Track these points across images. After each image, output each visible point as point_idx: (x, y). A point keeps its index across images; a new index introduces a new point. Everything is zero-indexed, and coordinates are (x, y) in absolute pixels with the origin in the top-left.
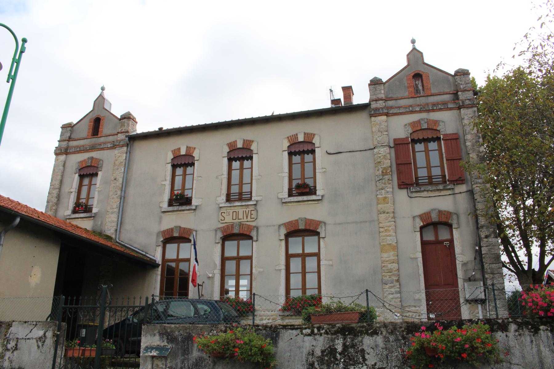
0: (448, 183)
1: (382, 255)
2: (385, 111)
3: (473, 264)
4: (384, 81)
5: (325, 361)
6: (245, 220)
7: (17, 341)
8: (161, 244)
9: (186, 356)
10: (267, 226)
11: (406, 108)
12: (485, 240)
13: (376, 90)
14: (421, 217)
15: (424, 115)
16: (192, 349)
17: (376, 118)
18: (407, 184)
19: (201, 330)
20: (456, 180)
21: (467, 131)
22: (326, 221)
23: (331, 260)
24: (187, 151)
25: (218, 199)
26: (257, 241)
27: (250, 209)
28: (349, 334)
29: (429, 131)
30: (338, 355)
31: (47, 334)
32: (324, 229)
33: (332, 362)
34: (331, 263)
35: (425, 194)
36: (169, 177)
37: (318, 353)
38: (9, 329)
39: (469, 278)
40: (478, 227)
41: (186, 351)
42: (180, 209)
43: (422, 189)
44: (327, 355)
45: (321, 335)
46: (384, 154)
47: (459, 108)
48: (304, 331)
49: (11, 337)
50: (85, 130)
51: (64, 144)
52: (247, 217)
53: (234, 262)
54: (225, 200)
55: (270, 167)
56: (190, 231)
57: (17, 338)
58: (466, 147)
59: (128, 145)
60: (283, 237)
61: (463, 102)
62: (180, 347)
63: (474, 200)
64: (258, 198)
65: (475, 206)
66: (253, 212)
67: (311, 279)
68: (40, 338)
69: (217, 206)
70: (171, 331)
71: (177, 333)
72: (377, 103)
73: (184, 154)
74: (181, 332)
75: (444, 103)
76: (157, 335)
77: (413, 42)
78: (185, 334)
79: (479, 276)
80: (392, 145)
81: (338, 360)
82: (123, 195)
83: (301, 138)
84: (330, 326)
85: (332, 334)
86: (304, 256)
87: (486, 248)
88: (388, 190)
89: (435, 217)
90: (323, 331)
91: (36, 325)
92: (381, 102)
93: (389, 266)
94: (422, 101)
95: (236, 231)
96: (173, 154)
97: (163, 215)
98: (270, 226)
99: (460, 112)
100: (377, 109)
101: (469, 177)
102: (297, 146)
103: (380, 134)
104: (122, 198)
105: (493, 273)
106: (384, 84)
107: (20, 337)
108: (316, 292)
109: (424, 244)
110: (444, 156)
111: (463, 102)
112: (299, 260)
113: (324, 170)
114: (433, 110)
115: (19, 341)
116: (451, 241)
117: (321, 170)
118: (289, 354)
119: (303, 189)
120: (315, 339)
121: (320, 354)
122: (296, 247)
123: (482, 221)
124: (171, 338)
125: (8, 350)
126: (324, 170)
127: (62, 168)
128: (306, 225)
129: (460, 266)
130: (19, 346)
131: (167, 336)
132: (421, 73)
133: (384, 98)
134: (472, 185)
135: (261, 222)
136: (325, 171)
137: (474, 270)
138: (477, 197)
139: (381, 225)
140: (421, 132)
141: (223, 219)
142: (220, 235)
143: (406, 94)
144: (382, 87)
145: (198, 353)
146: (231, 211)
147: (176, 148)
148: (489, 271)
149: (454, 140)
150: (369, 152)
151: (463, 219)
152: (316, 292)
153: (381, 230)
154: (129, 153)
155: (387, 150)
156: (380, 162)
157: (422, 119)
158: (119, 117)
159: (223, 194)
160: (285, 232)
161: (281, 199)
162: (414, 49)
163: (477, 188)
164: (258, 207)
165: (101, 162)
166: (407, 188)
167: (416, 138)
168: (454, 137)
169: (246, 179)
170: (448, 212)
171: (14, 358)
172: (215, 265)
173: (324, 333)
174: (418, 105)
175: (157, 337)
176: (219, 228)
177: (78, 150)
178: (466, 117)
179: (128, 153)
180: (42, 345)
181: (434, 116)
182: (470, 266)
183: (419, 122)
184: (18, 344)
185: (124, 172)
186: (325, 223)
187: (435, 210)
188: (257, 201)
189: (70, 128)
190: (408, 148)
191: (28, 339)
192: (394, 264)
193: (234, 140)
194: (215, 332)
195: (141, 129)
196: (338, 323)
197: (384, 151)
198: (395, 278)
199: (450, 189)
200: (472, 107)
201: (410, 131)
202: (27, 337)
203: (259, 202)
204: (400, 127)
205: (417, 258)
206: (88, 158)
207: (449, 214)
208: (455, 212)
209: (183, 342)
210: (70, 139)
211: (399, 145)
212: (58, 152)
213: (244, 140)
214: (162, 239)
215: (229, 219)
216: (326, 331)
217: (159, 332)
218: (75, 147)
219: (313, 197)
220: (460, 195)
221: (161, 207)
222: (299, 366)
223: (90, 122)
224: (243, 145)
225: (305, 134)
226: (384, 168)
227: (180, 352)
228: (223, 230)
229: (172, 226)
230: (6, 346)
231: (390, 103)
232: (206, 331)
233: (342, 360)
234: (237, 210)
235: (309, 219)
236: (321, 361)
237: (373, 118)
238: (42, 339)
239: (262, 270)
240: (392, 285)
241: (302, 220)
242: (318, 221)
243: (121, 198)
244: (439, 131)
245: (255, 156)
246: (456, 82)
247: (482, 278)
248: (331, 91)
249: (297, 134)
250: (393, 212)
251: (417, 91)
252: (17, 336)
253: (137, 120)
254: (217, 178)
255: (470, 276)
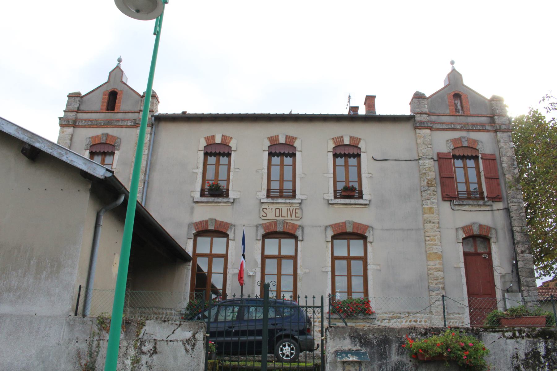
0: (486, 199)
1: (428, 263)
2: (430, 125)
3: (511, 276)
4: (427, 95)
5: (530, 365)
6: (289, 218)
7: (156, 343)
8: (192, 236)
9: (384, 361)
10: (313, 226)
11: (448, 124)
12: (521, 255)
13: (420, 104)
14: (463, 229)
15: (464, 134)
16: (390, 354)
17: (421, 130)
18: (451, 197)
19: (398, 332)
20: (495, 198)
21: (503, 154)
22: (374, 226)
23: (379, 265)
24: (222, 139)
25: (258, 193)
26: (302, 241)
27: (294, 208)
28: (550, 338)
29: (469, 150)
30: (541, 358)
31: (197, 336)
32: (371, 233)
33: (536, 365)
34: (378, 267)
35: (466, 208)
36: (201, 166)
37: (522, 356)
38: (142, 328)
39: (507, 289)
40: (514, 243)
41: (384, 356)
42: (216, 201)
43: (465, 203)
44: (531, 358)
45: (523, 338)
46: (429, 166)
47: (496, 131)
48: (506, 334)
49: (145, 338)
50: (99, 103)
51: (72, 115)
52: (291, 216)
53: (345, 262)
54: (266, 196)
55: (314, 165)
56: (227, 225)
57: (155, 340)
58: (502, 168)
59: (152, 125)
60: (329, 239)
61: (500, 126)
62: (375, 351)
63: (510, 217)
64: (303, 197)
65: (511, 223)
66: (297, 211)
67: (357, 283)
68: (188, 341)
69: (259, 201)
70: (364, 334)
71: (371, 336)
72: (421, 116)
73: (219, 142)
74: (376, 335)
75: (483, 125)
76: (348, 338)
77: (452, 63)
78: (381, 337)
79: (515, 288)
80: (436, 159)
81: (542, 364)
82: (147, 179)
83: (347, 141)
84: (531, 330)
85: (534, 337)
86: (279, 258)
87: (522, 263)
88: (433, 201)
89: (476, 231)
90: (524, 335)
91: (180, 325)
92: (425, 116)
93: (436, 273)
94: (462, 120)
95: (280, 228)
96: (206, 141)
97: (195, 205)
98: (316, 226)
99: (496, 135)
100: (421, 122)
101: (504, 195)
102: (342, 148)
103: (424, 146)
104: (146, 183)
105: (528, 286)
106: (427, 99)
107: (158, 339)
108: (362, 296)
109: (466, 254)
110: (482, 174)
111: (500, 126)
112: (345, 262)
113: (370, 175)
114: (472, 130)
115: (158, 343)
116: (490, 254)
117: (367, 175)
118: (494, 357)
119: (349, 192)
120: (517, 342)
121: (524, 357)
122: (341, 249)
123: (518, 237)
124: (365, 342)
125: (144, 353)
126: (370, 175)
127: (69, 142)
128: (353, 228)
129: (499, 278)
130: (158, 349)
131: (360, 340)
132: (460, 93)
133: (428, 112)
134: (508, 204)
135: (304, 222)
136: (371, 176)
137: (511, 282)
138: (512, 214)
139: (427, 234)
140: (461, 149)
141: (265, 215)
142: (262, 232)
143: (448, 112)
144: (425, 101)
145: (397, 357)
146: (274, 208)
147: (210, 135)
148: (525, 284)
149: (491, 160)
150: (414, 162)
151: (501, 234)
152: (362, 296)
153: (427, 238)
154: (154, 134)
155: (432, 163)
156: (425, 174)
157: (464, 138)
158: (142, 94)
159: (264, 189)
160: (333, 234)
161: (328, 200)
162: (454, 70)
163: (513, 207)
164: (303, 206)
165: (119, 140)
166: (450, 201)
167: (457, 155)
168: (492, 157)
169: (288, 175)
170: (487, 227)
171: (155, 363)
172: (256, 263)
173: (526, 336)
174: (459, 124)
175: (348, 341)
176: (260, 225)
177: (90, 123)
178: (502, 141)
179: (153, 134)
180: (192, 349)
181: (473, 135)
182: (508, 278)
183: (460, 139)
184: (158, 346)
185: (148, 155)
186: (372, 228)
187: (476, 223)
188: (302, 200)
189: (79, 99)
190: (451, 162)
191: (171, 341)
192: (439, 272)
193: (276, 135)
194: (414, 334)
195: (163, 109)
196: (538, 327)
197: (429, 163)
198: (441, 286)
199: (489, 205)
200: (507, 132)
201: (452, 147)
202: (169, 339)
203: (304, 201)
204: (442, 142)
205: (460, 268)
206: (103, 134)
207: (489, 229)
208: (494, 227)
209: (379, 345)
210: (78, 111)
211: (441, 159)
212: (64, 123)
213: (287, 136)
214: (195, 232)
215: (271, 216)
216: (527, 334)
217: (350, 335)
218: (85, 120)
219: (361, 201)
220: (497, 211)
221: (193, 198)
222: (505, 369)
223: (104, 94)
224: (286, 141)
225: (351, 137)
226: (429, 180)
227: (376, 356)
228: (265, 226)
229: (207, 219)
230: (140, 348)
231: (433, 118)
232: (405, 334)
233: (547, 364)
234: (280, 208)
235: (356, 223)
236: (526, 364)
237: (418, 131)
238: (191, 342)
239: (307, 271)
240: (438, 292)
241: (349, 223)
242: (366, 226)
243: (144, 183)
244: (478, 150)
245: (298, 154)
246: (492, 106)
247: (518, 289)
248: (349, 97)
249: (342, 137)
250: (438, 223)
251: (457, 110)
252: (154, 337)
253: (159, 100)
254: (257, 171)
255: (508, 287)
